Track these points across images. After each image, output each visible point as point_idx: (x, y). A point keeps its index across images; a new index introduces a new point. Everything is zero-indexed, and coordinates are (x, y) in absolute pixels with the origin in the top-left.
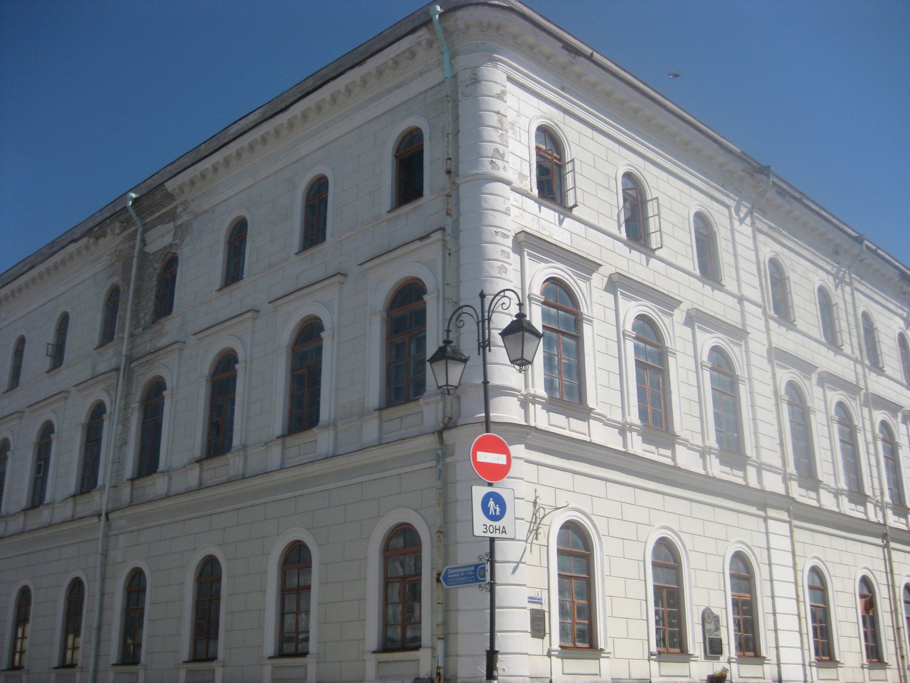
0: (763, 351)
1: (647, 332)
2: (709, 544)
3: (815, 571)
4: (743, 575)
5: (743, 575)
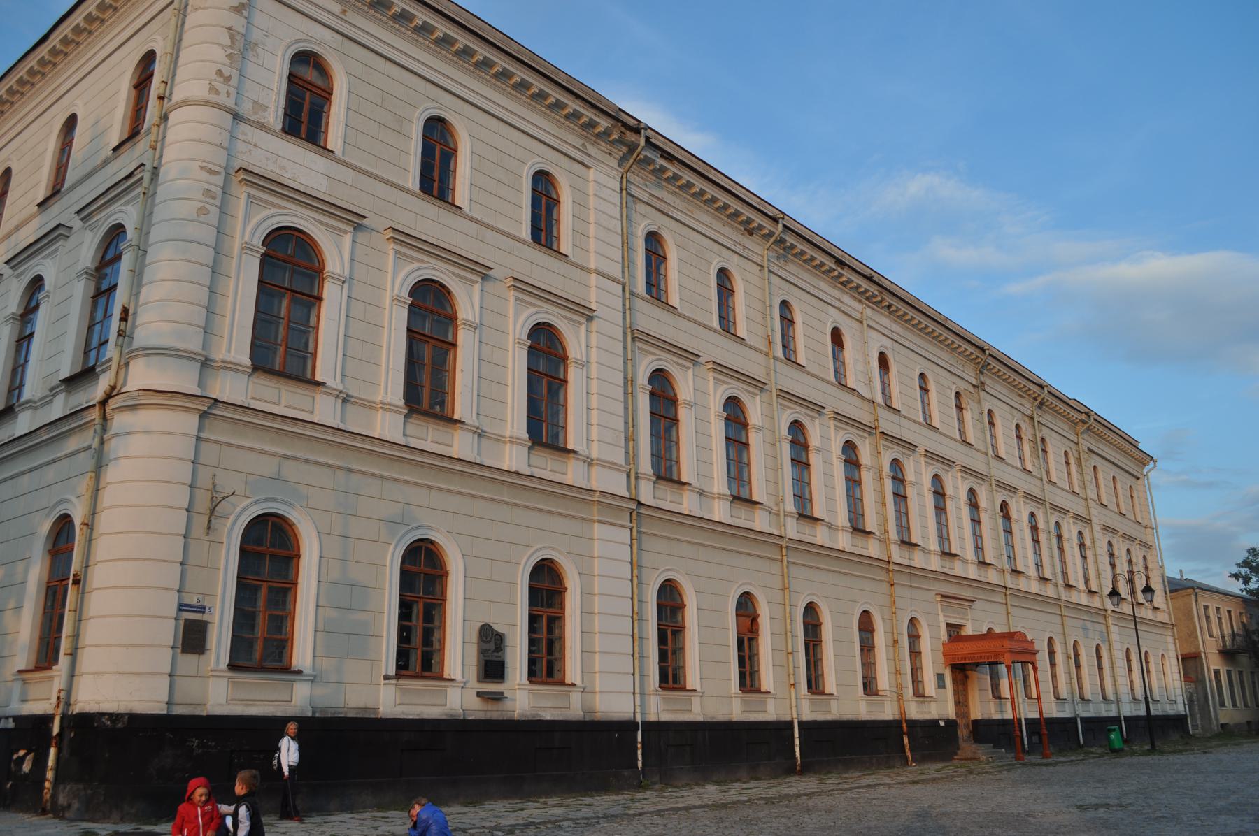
4: (546, 586)
5: (546, 586)
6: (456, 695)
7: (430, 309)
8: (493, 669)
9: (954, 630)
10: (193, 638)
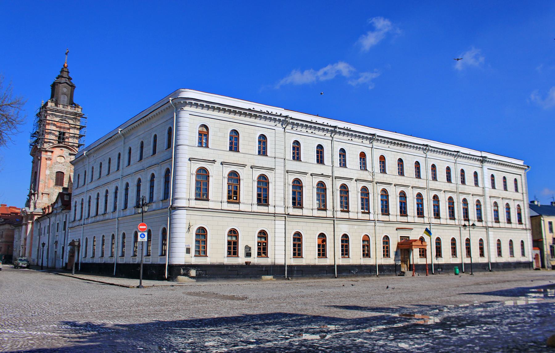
4: (263, 234)
6: (241, 259)
7: (234, 177)
10: (188, 251)
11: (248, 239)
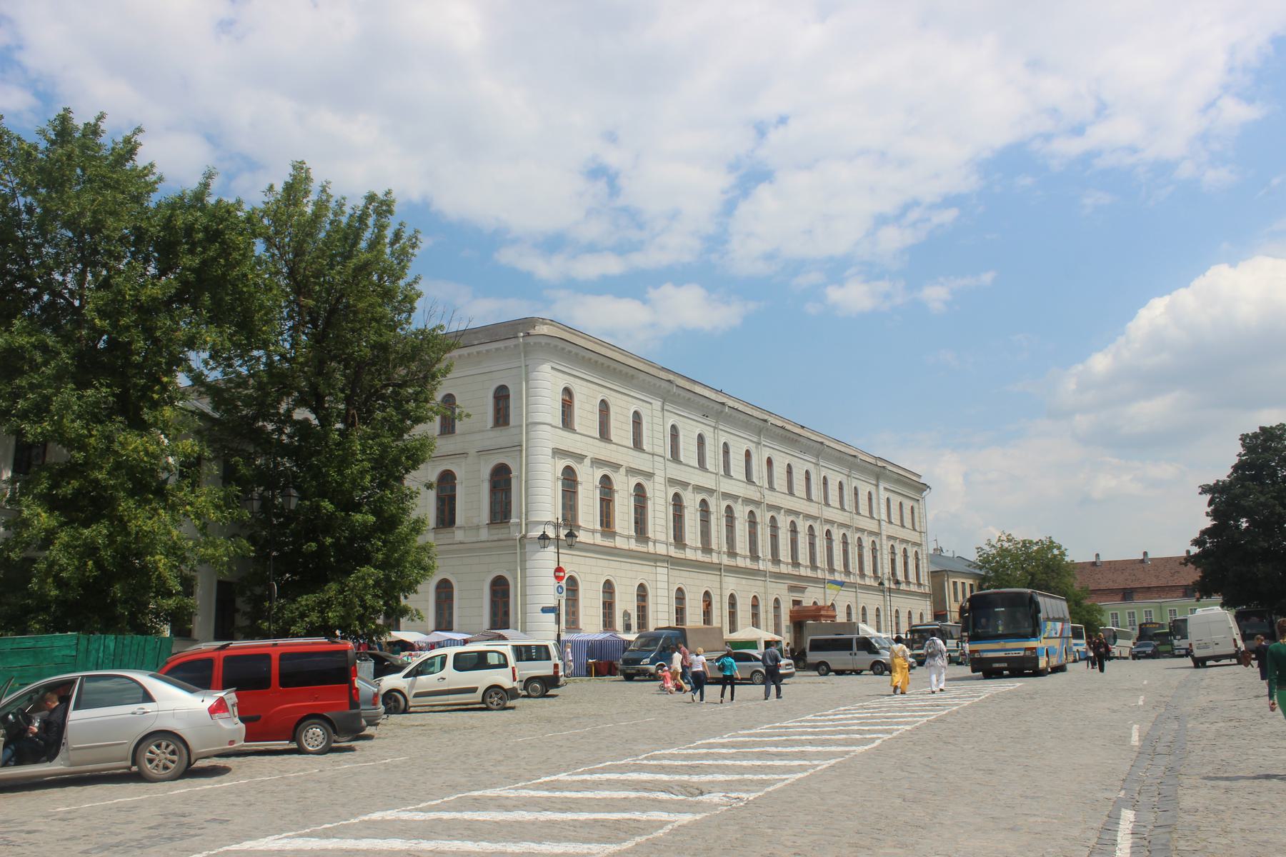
0: (662, 481)
1: (606, 481)
2: (626, 581)
3: (680, 590)
4: (642, 593)
5: (642, 593)
8: (628, 628)
9: (796, 603)
11: (625, 602)
